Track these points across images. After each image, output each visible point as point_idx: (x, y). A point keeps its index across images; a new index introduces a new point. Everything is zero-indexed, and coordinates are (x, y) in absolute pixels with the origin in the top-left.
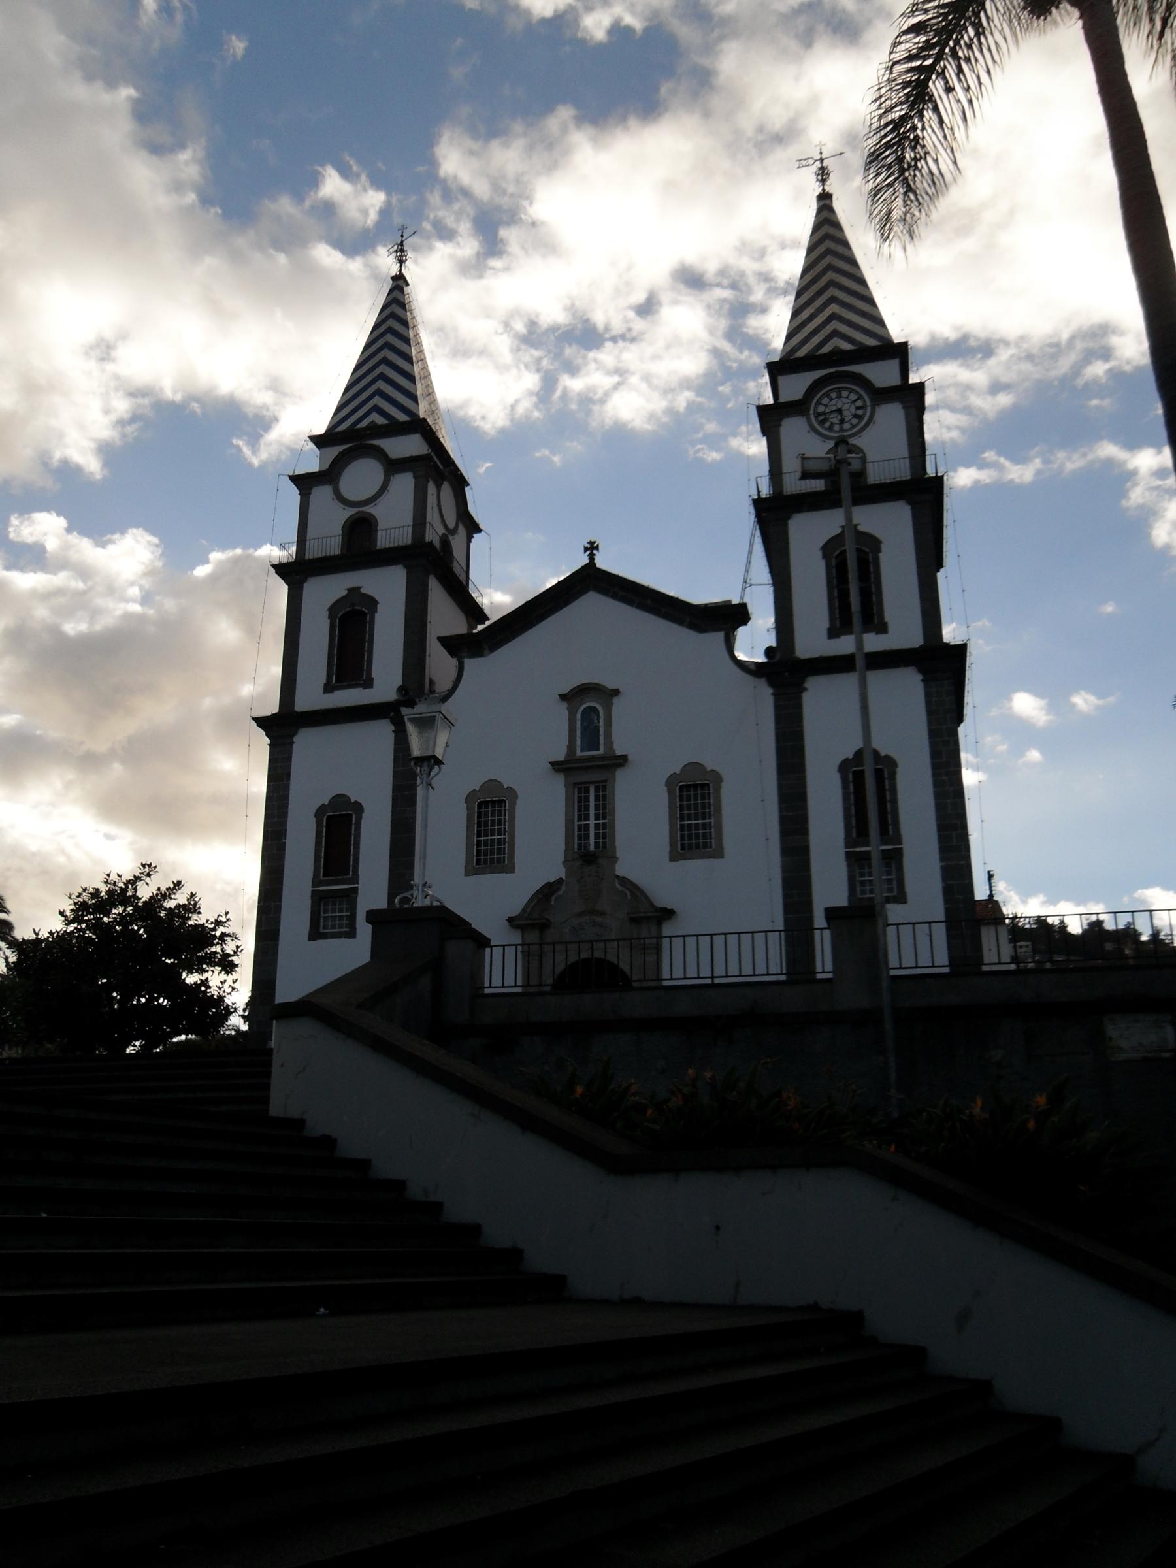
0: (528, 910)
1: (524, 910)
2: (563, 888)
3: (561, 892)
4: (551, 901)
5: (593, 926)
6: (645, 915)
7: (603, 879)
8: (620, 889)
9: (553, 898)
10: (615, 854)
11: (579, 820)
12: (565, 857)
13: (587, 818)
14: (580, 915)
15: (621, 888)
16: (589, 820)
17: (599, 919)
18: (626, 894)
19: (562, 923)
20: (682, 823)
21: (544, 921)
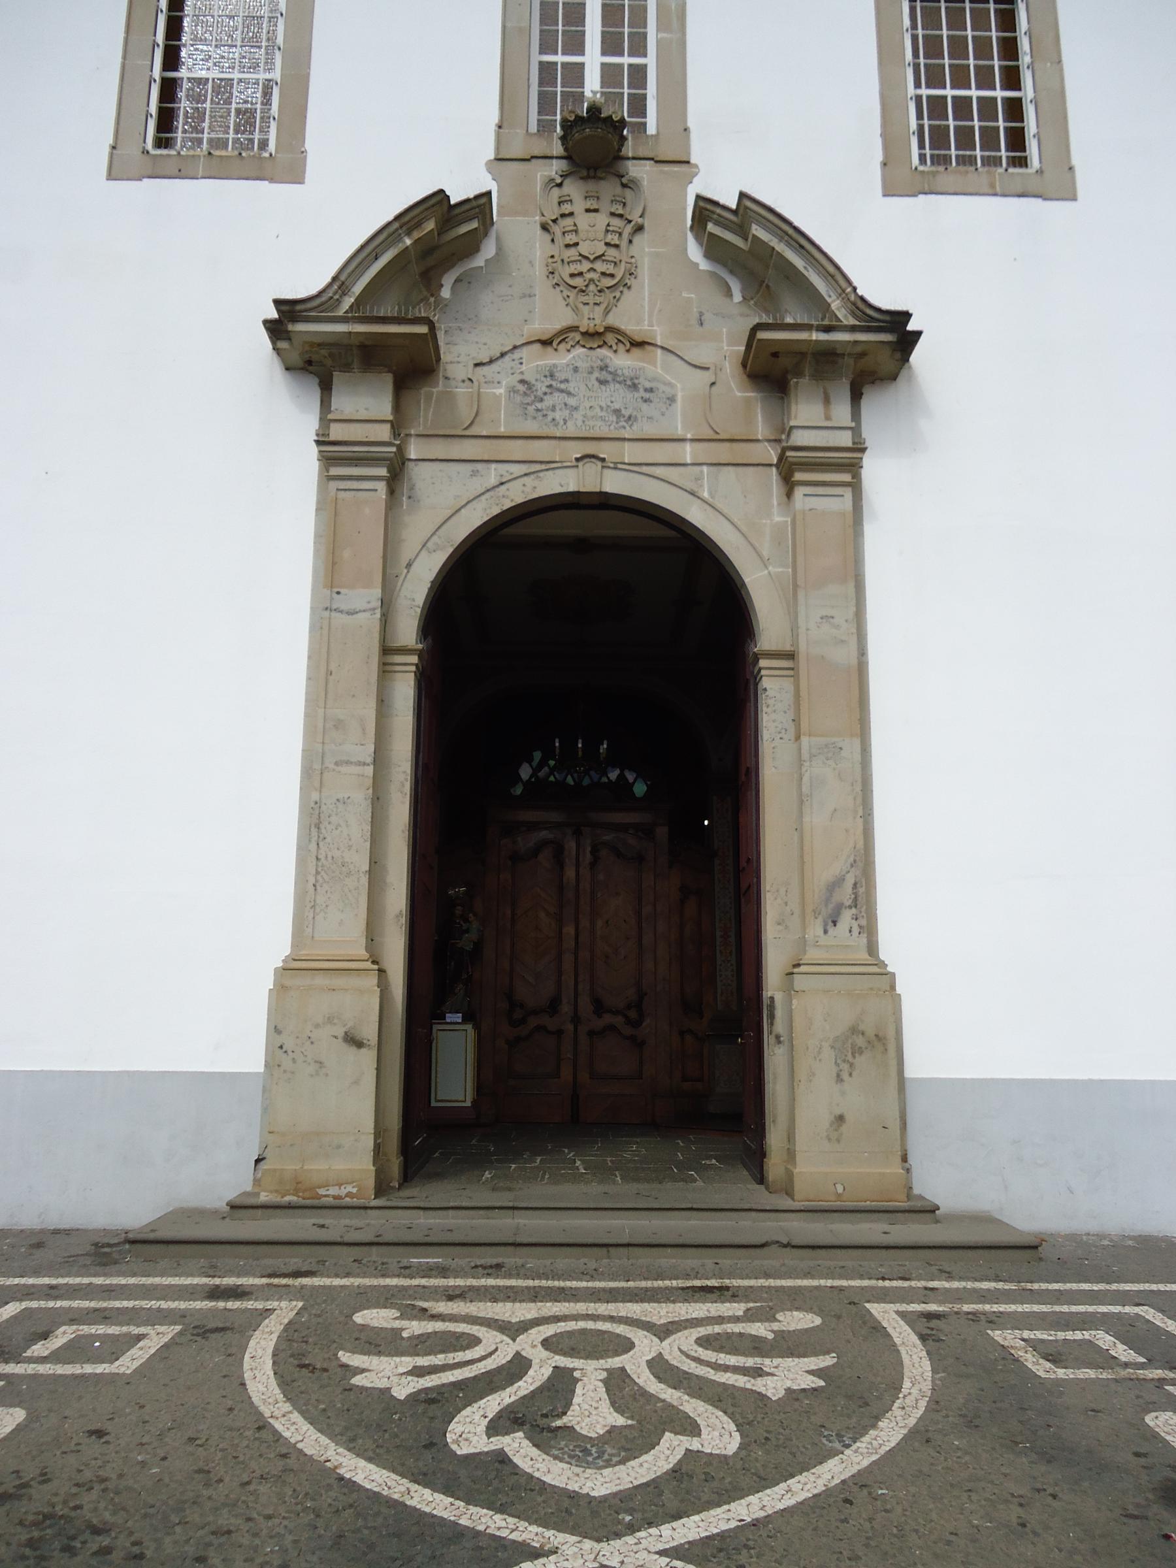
0: (358, 288)
1: (340, 282)
2: (489, 250)
3: (479, 261)
4: (442, 286)
5: (602, 382)
6: (823, 337)
7: (640, 229)
8: (702, 267)
9: (448, 280)
10: (689, 154)
11: (547, 46)
12: (498, 149)
13: (576, 44)
14: (546, 343)
15: (704, 265)
16: (582, 52)
17: (623, 361)
18: (729, 293)
19: (476, 365)
20: (919, 92)
21: (423, 329)
